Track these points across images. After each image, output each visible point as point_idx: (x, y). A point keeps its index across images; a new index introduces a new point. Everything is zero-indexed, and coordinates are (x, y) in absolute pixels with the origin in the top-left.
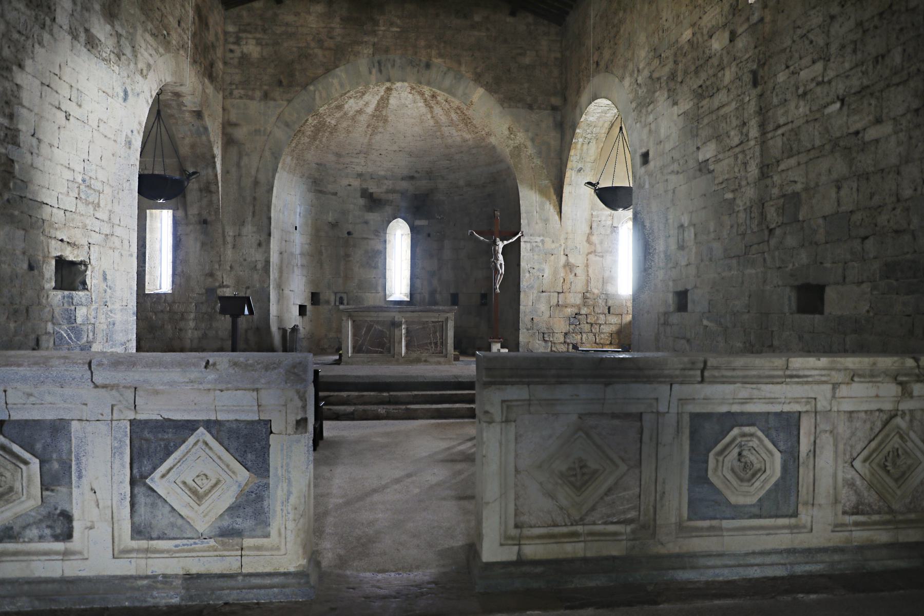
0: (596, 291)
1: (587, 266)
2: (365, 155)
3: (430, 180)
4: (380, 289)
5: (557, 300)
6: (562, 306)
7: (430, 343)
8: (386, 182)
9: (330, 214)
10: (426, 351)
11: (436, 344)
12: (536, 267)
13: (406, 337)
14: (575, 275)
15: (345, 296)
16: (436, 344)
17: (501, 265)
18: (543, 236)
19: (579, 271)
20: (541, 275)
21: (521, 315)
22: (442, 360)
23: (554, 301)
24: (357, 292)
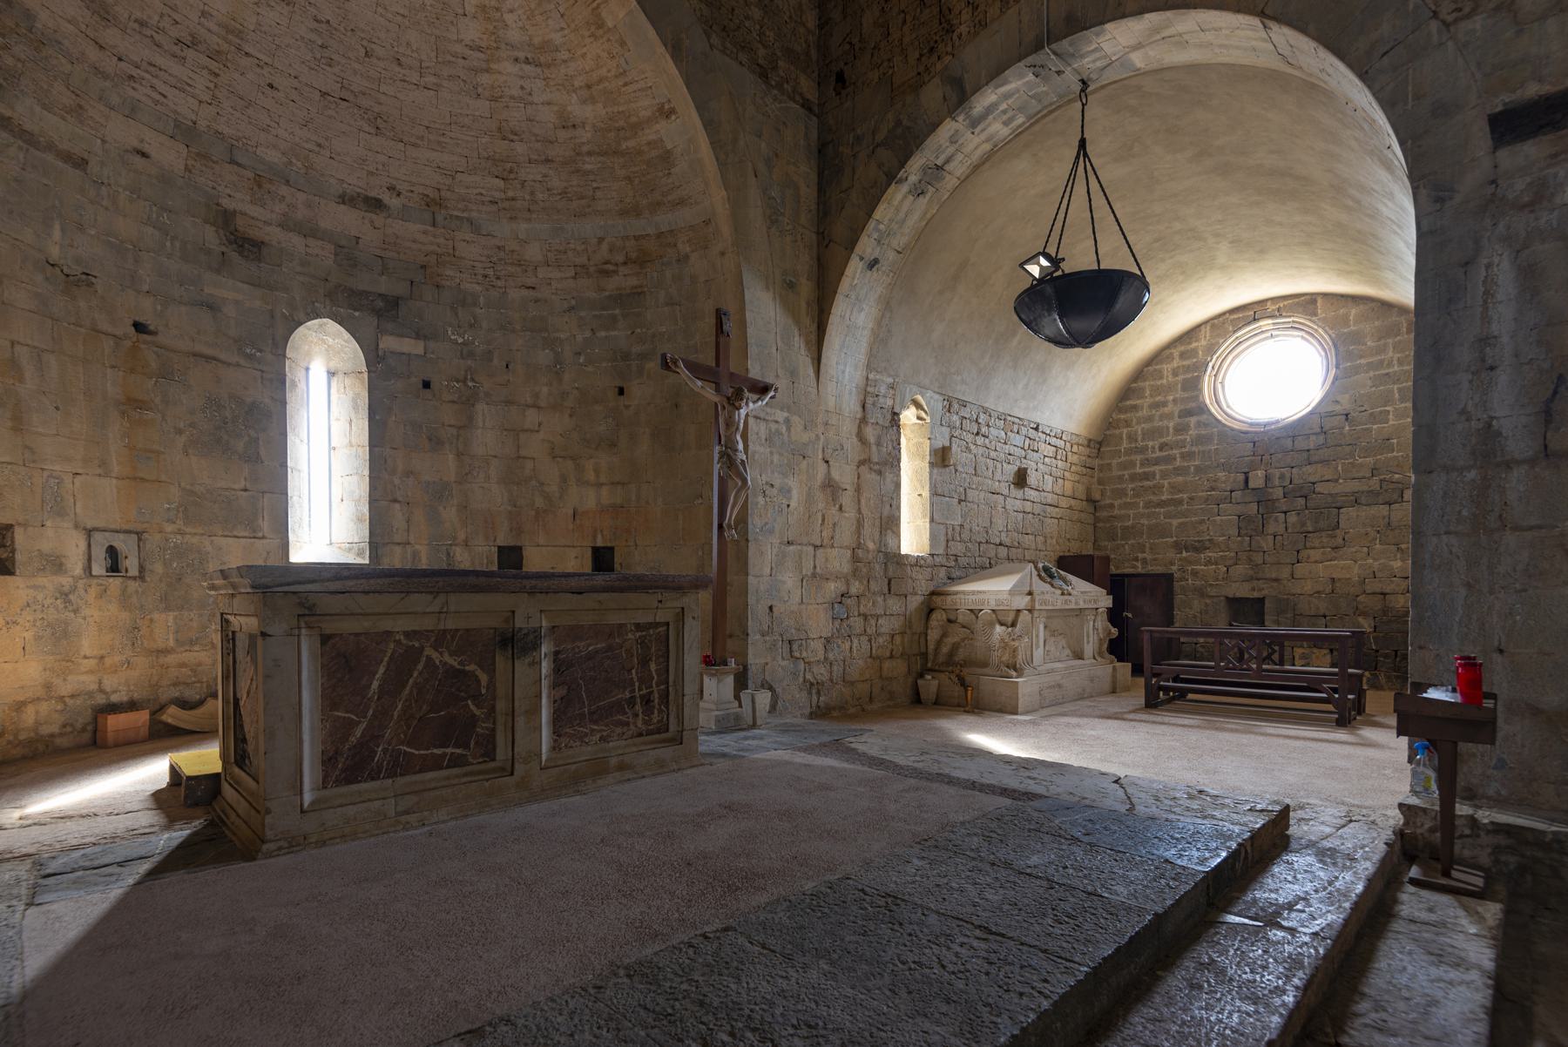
0: (871, 546)
2: (213, 65)
3: (434, 225)
4: (265, 525)
6: (821, 577)
7: (631, 702)
8: (284, 190)
9: (57, 233)
10: (619, 730)
11: (647, 700)
12: (777, 483)
13: (554, 686)
14: (841, 508)
15: (125, 545)
16: (647, 700)
18: (788, 411)
21: (751, 600)
22: (666, 752)
23: (807, 569)
24: (181, 533)
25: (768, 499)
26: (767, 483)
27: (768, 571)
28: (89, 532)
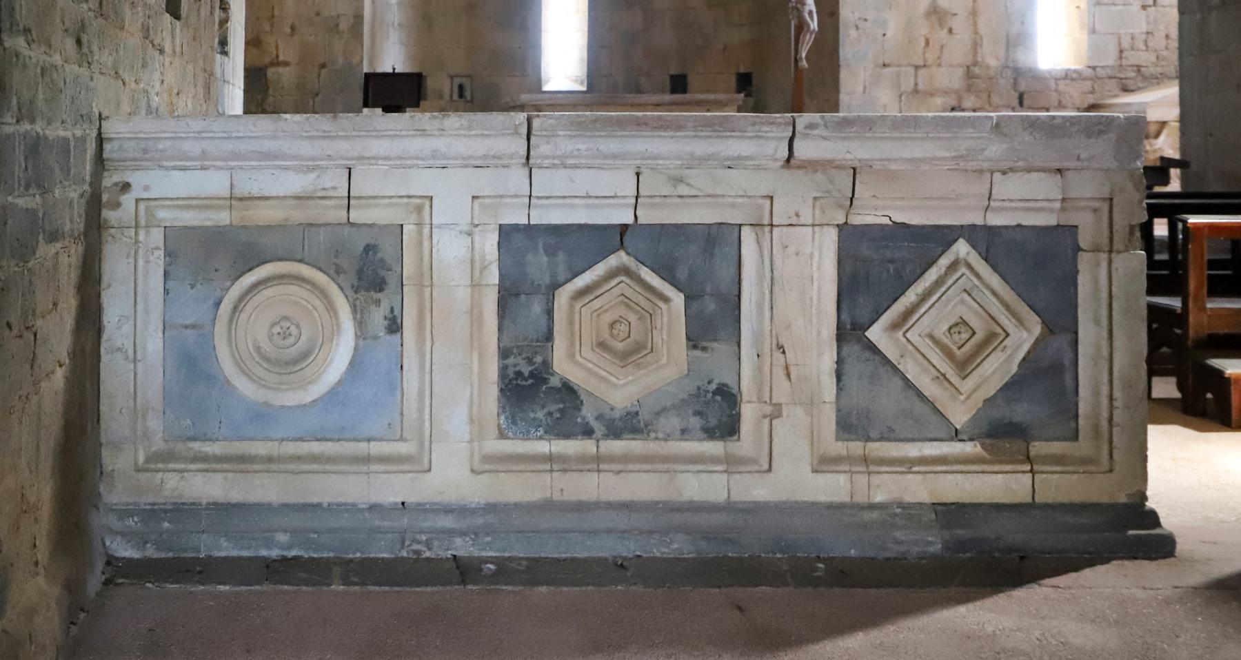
0: (992, 62)
1: (974, 13)
5: (912, 82)
12: (870, 17)
14: (950, 31)
15: (467, 84)
17: (810, 13)
19: (956, 23)
20: (881, 32)
23: (908, 85)
25: (861, 31)
26: (860, 19)
27: (861, 89)
28: (452, 77)
